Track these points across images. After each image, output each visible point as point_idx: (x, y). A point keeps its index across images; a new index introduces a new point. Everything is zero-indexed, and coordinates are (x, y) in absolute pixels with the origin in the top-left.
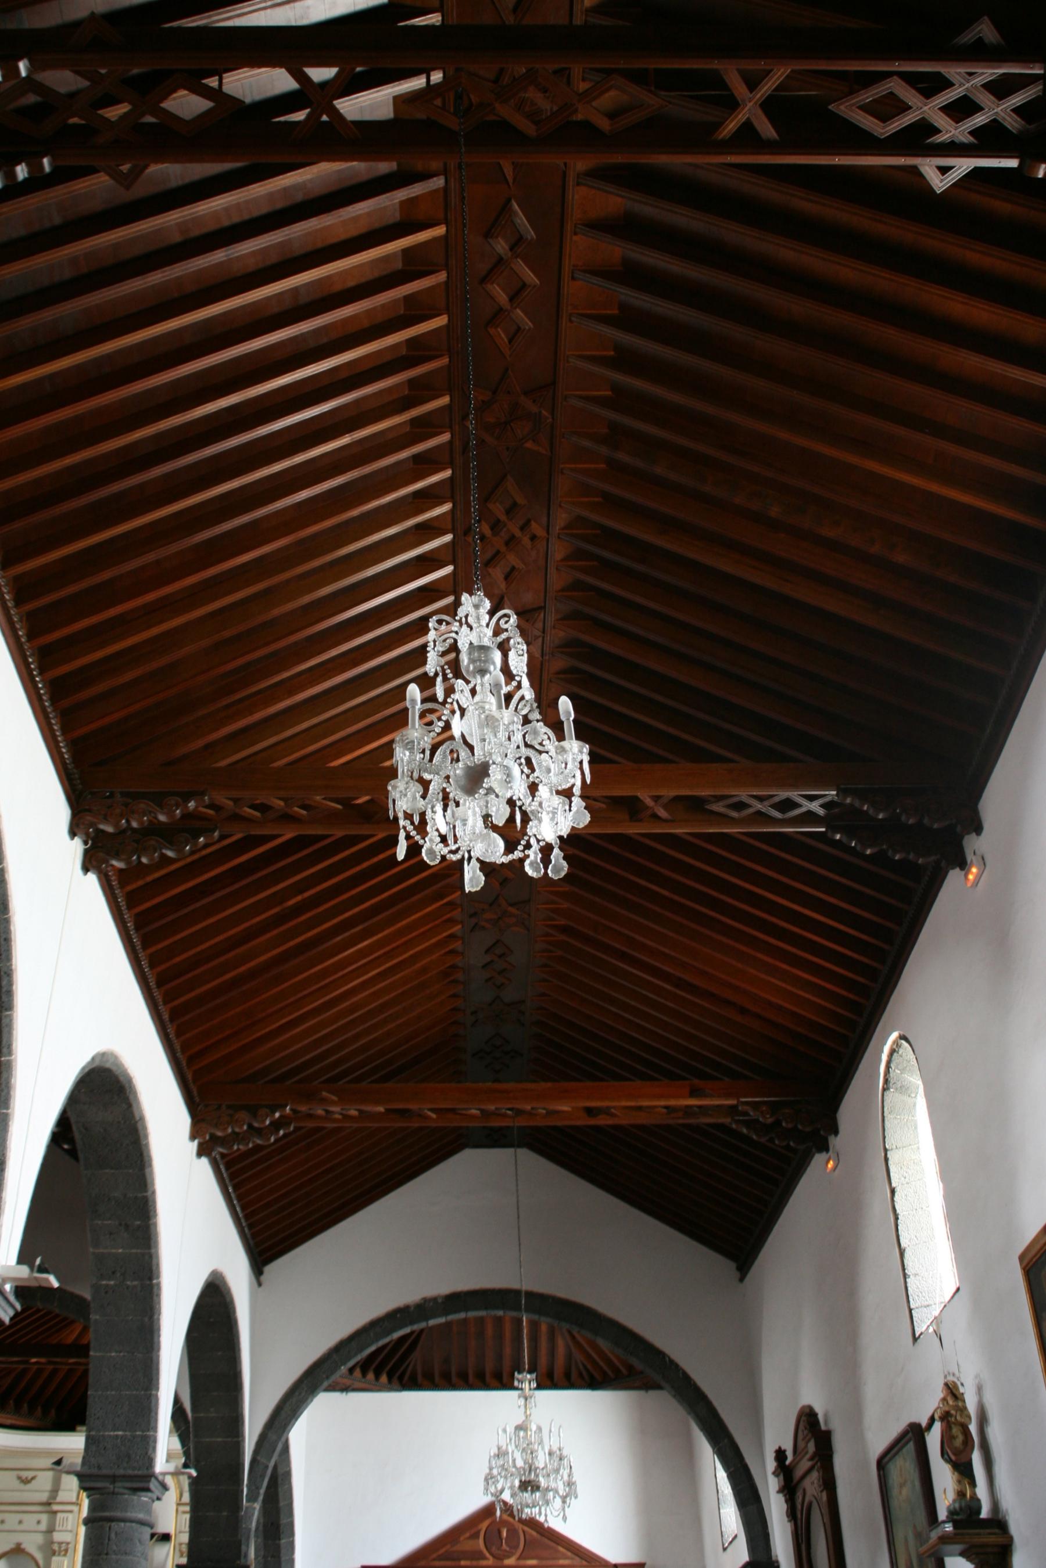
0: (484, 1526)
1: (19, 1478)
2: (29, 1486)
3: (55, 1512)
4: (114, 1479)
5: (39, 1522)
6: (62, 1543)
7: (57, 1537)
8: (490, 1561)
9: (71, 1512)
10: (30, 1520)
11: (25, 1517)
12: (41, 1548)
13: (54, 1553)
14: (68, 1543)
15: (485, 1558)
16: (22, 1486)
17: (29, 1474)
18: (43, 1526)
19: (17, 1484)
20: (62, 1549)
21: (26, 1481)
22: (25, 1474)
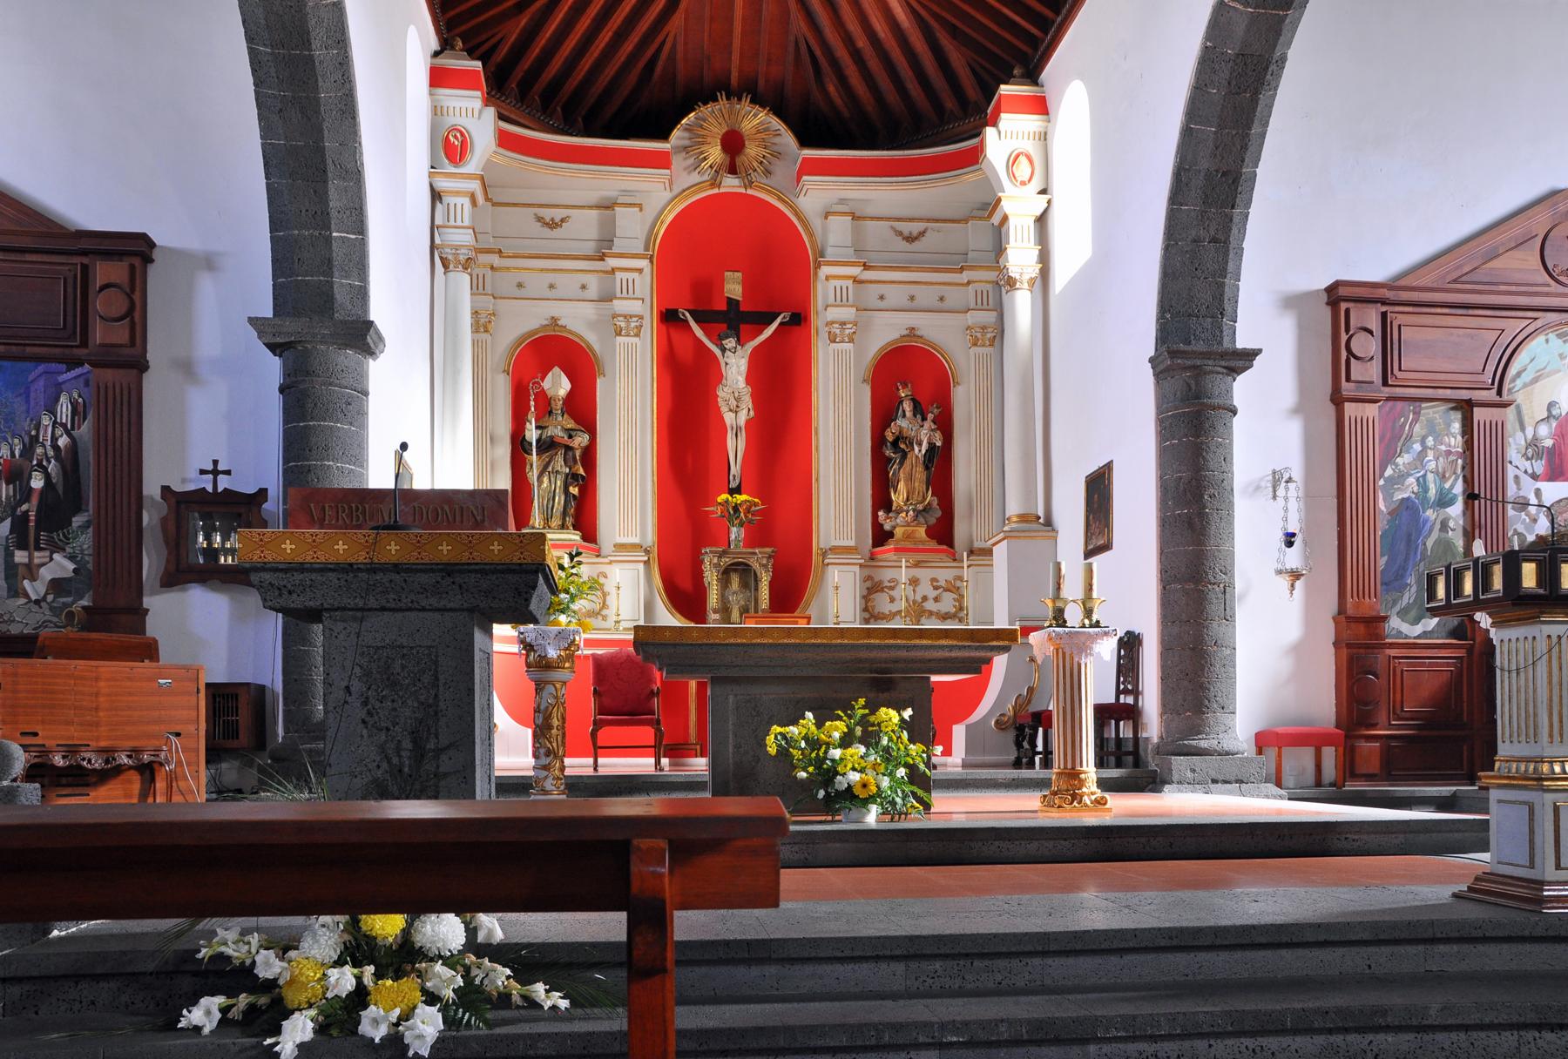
1: (540, 219)
2: (557, 233)
3: (613, 271)
5: (584, 287)
6: (631, 317)
7: (620, 306)
9: (640, 271)
10: (568, 284)
12: (592, 325)
13: (619, 334)
14: (641, 317)
16: (547, 232)
17: (558, 214)
18: (592, 292)
20: (633, 325)
21: (553, 225)
22: (548, 214)
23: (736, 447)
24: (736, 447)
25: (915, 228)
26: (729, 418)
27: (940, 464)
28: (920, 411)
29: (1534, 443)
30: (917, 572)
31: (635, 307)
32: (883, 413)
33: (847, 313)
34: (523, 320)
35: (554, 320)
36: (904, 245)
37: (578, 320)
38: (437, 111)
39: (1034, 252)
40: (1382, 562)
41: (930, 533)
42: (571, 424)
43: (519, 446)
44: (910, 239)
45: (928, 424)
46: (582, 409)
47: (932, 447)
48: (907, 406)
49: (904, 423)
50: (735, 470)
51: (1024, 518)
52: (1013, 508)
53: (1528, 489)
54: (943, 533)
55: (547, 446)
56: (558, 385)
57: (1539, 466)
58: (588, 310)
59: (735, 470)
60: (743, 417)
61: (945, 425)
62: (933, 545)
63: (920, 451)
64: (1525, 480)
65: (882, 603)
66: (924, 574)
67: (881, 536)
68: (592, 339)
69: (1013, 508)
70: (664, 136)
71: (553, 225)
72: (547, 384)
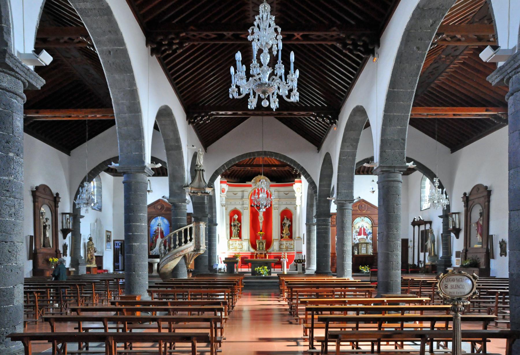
0: (358, 204)
4: (346, 201)
7: (245, 206)
8: (359, 212)
10: (237, 203)
11: (236, 202)
15: (358, 211)
17: (236, 193)
18: (241, 204)
19: (233, 195)
21: (235, 194)
22: (234, 193)
23: (261, 225)
24: (261, 225)
25: (287, 193)
26: (260, 221)
27: (290, 227)
28: (287, 219)
29: (357, 231)
30: (287, 242)
31: (247, 206)
32: (282, 219)
33: (277, 206)
34: (231, 208)
35: (236, 208)
36: (285, 195)
37: (239, 208)
38: (221, 186)
39: (300, 201)
40: (336, 246)
41: (289, 237)
42: (238, 222)
43: (231, 226)
44: (286, 194)
45: (289, 221)
46: (239, 220)
47: (289, 225)
48: (286, 219)
49: (285, 221)
50: (261, 228)
51: (298, 237)
52: (297, 236)
53: (356, 237)
54: (291, 237)
55: (235, 226)
56: (236, 217)
57: (357, 234)
58: (240, 206)
59: (261, 228)
60: (262, 221)
61: (291, 221)
62: (289, 239)
63: (287, 225)
64: (356, 236)
65: (282, 247)
66: (288, 243)
67: (282, 237)
68: (241, 210)
69: (297, 236)
70: (250, 181)
71: (235, 194)
72: (234, 217)
